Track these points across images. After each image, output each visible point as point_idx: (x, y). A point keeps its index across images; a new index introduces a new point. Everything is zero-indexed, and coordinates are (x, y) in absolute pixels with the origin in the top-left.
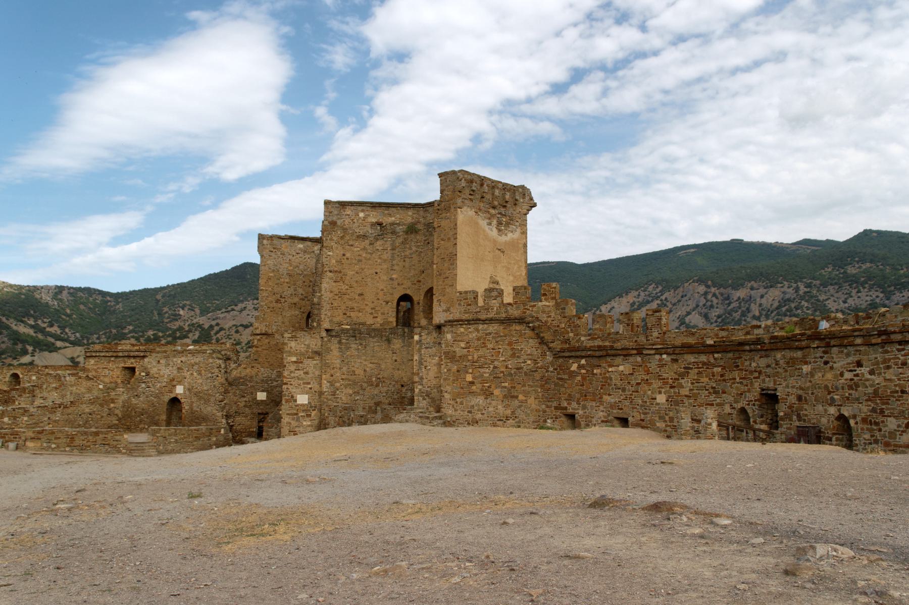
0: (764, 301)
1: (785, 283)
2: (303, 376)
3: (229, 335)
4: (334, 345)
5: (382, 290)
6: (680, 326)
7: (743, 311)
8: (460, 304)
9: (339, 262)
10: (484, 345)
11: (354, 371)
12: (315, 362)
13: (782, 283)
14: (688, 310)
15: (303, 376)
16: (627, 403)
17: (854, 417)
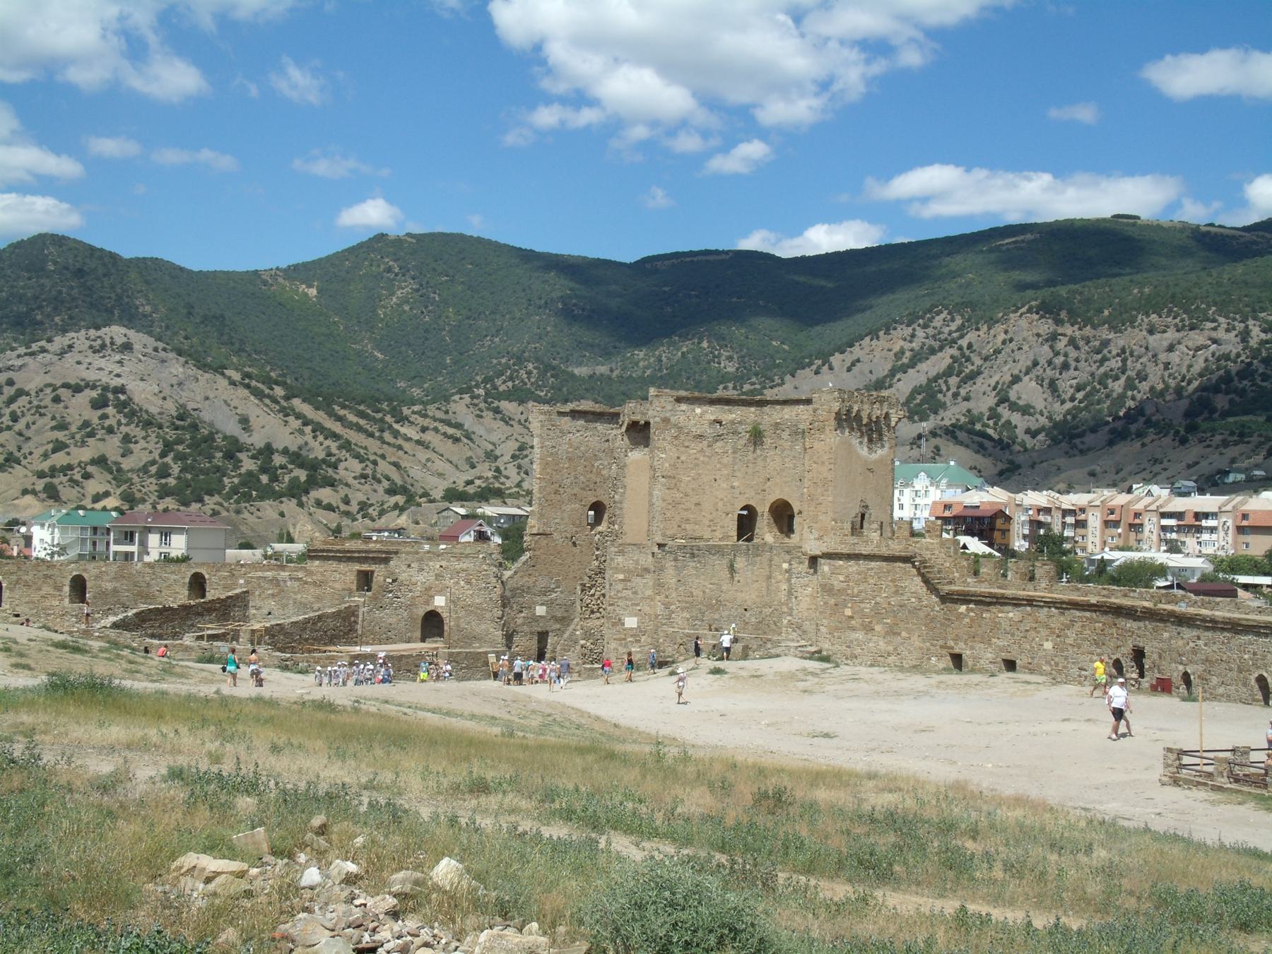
0: (1174, 357)
1: (1222, 320)
2: (632, 596)
3: (39, 407)
4: (669, 564)
5: (722, 500)
6: (997, 405)
7: (1128, 378)
8: (835, 534)
9: (674, 466)
10: (865, 580)
11: (691, 593)
12: (645, 581)
13: (1214, 321)
14: (1016, 372)
15: (632, 596)
16: (1016, 647)
17: (1194, 674)
